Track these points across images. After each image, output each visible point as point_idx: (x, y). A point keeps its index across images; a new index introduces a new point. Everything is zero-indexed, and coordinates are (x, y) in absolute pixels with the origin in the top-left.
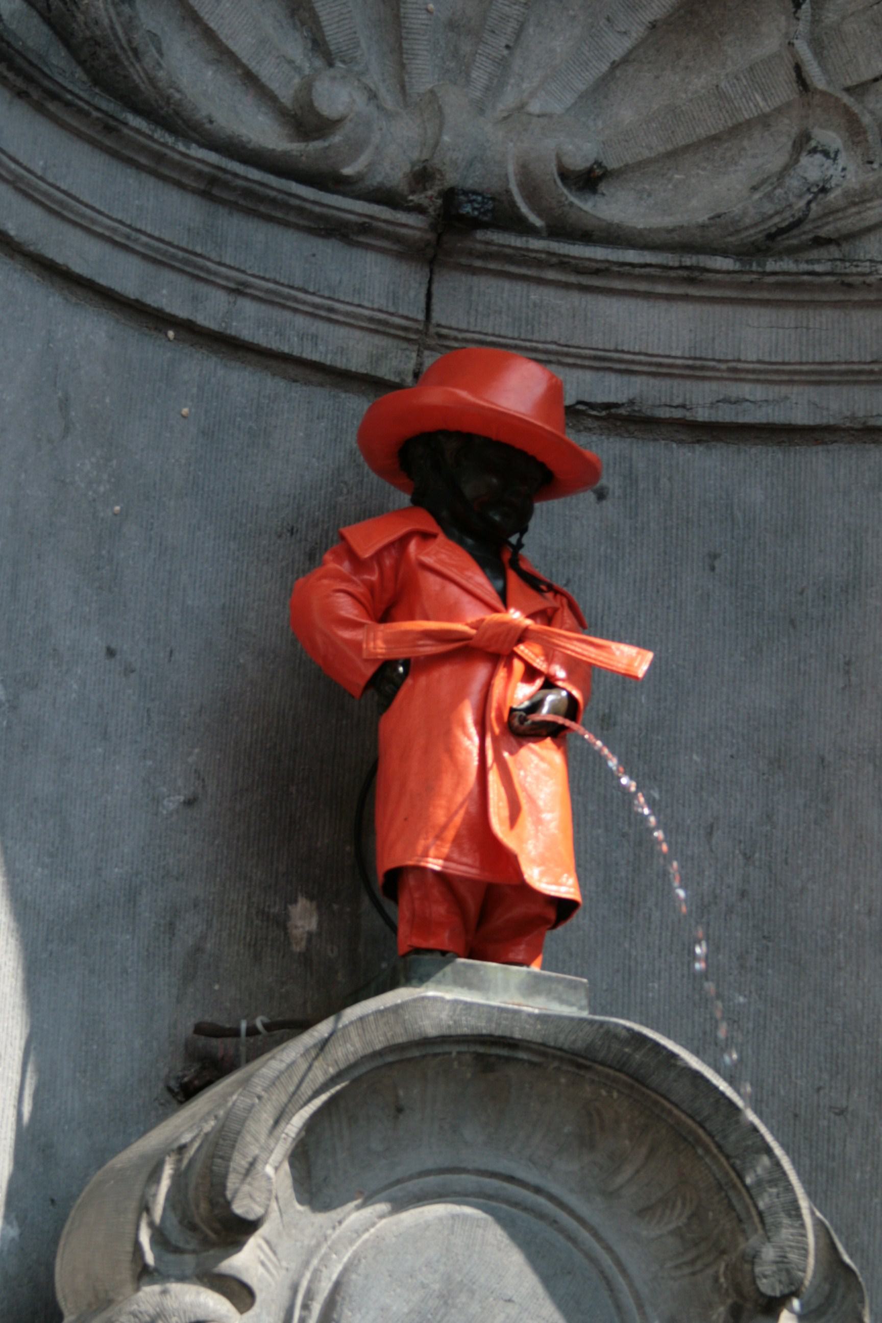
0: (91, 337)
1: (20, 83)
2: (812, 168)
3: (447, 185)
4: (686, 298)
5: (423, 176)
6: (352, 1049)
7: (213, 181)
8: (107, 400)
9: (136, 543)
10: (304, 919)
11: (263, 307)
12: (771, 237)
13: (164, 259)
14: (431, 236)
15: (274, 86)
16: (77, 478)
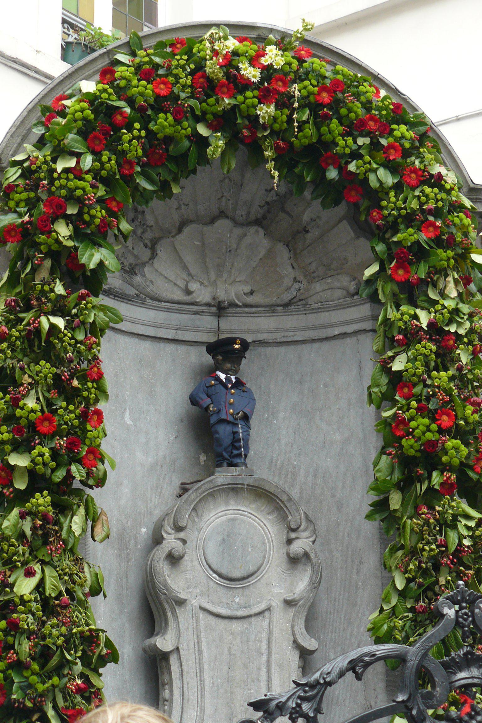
1: (121, 300)
2: (297, 286)
3: (220, 300)
4: (273, 316)
5: (214, 299)
7: (168, 308)
10: (203, 458)
12: (290, 301)
14: (217, 311)
15: (181, 285)
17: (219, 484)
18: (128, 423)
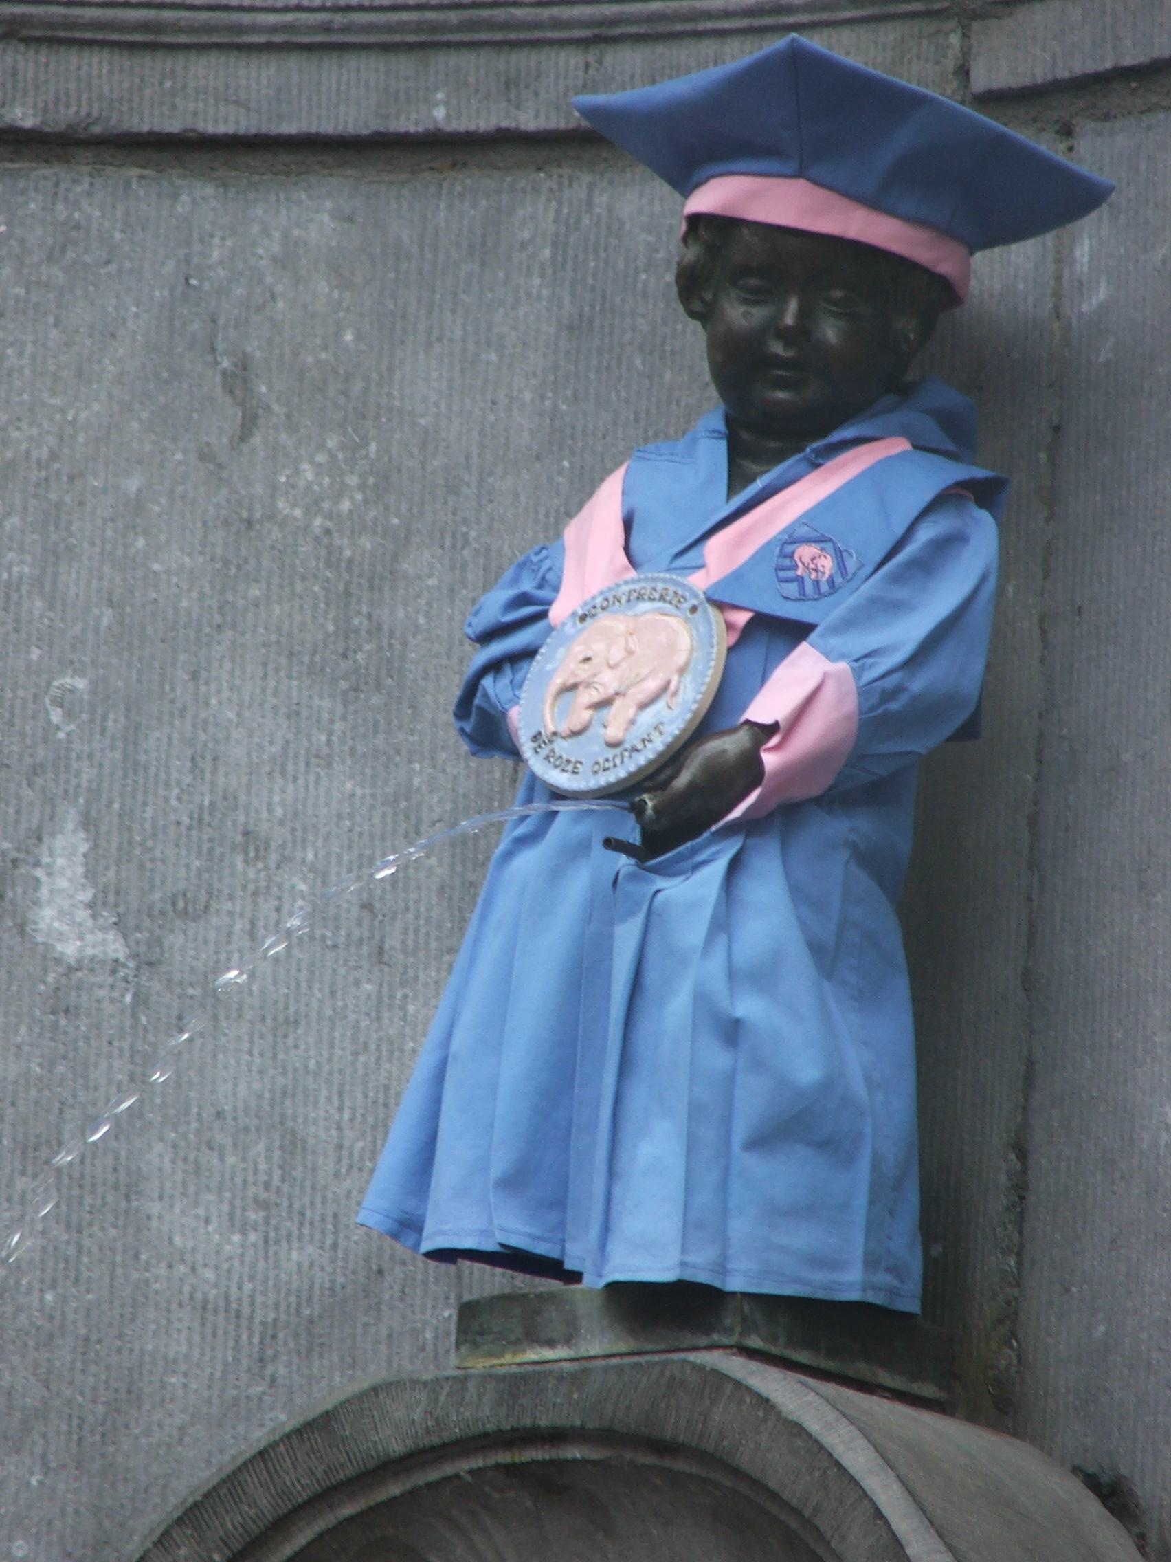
0: (296, 232)
6: (252, 1512)
8: (349, 337)
9: (430, 582)
11: (660, 49)
13: (423, 38)
16: (281, 504)
17: (397, 1447)
18: (69, 949)
